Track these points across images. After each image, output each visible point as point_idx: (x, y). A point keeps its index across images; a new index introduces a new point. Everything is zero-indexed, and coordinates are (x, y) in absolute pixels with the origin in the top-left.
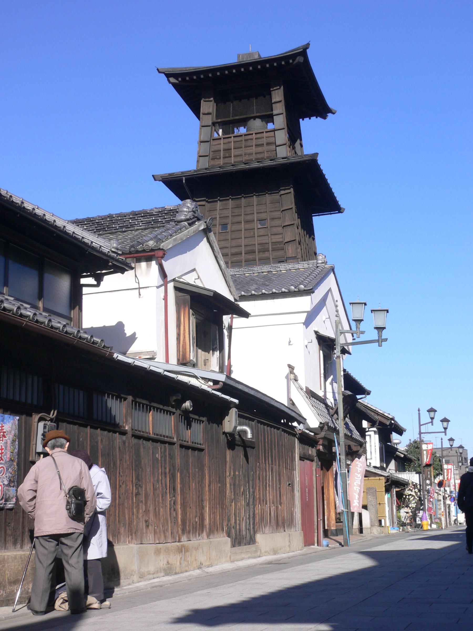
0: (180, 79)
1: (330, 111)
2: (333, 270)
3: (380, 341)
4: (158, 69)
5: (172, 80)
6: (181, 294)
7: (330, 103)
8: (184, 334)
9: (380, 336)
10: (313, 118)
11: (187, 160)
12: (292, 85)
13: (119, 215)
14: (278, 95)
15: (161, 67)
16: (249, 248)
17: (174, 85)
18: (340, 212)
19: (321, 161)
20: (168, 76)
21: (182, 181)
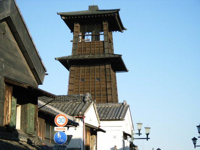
0: (66, 18)
1: (123, 29)
2: (128, 106)
3: (147, 139)
4: (57, 13)
5: (63, 18)
6: (87, 128)
7: (125, 26)
8: (88, 141)
9: (147, 136)
10: (117, 31)
11: (67, 52)
12: (111, 21)
13: (63, 96)
14: (105, 28)
15: (59, 12)
16: (93, 89)
17: (64, 20)
18: (126, 72)
19: (123, 58)
20: (62, 16)
21: (67, 61)
